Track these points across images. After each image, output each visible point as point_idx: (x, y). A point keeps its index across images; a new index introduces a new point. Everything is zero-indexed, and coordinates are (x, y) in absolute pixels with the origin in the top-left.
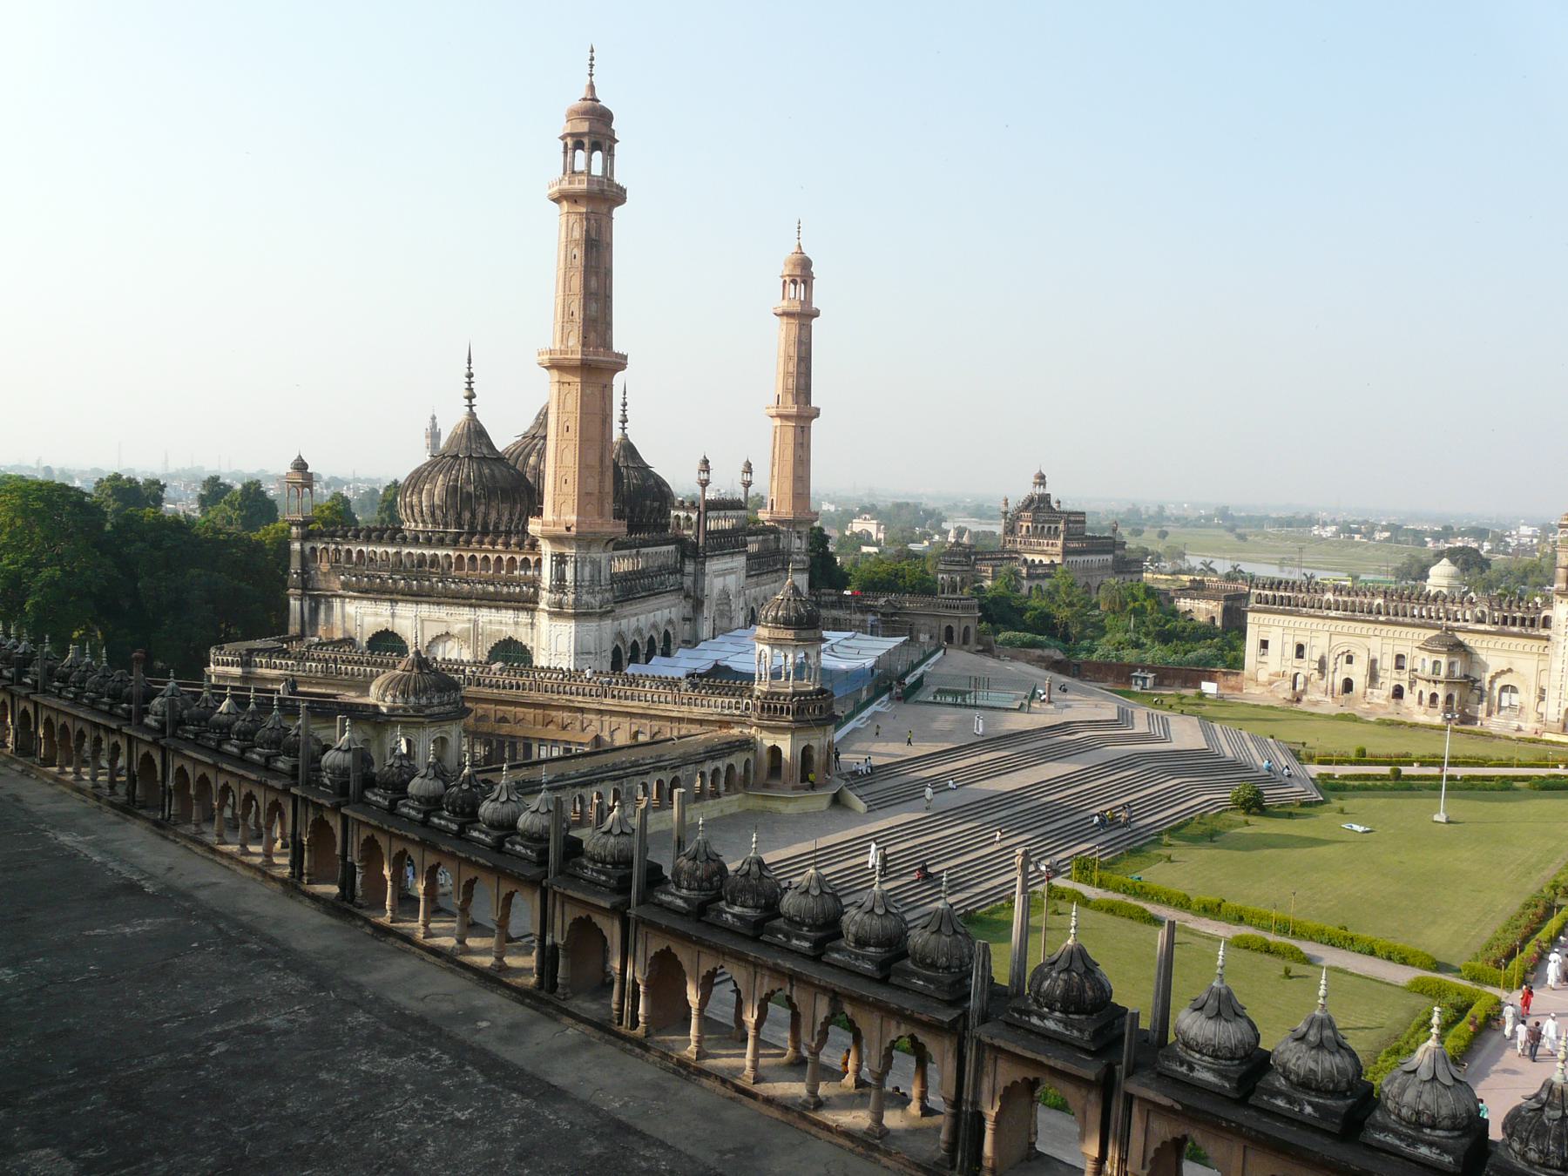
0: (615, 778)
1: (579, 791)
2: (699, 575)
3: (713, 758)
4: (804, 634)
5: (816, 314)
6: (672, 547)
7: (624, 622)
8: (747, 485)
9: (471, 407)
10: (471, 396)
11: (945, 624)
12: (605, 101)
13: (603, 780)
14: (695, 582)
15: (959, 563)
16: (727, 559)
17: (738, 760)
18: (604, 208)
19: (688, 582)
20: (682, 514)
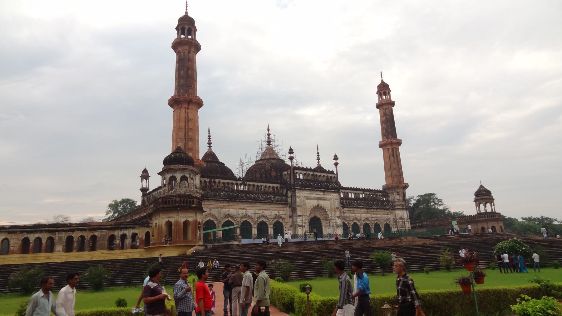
0: (49, 231)
1: (25, 235)
2: (294, 196)
3: (121, 229)
4: (172, 167)
5: (393, 104)
6: (276, 185)
7: (231, 210)
8: (336, 164)
9: (210, 147)
10: (210, 144)
11: (480, 227)
12: (190, 15)
13: (41, 232)
14: (292, 200)
15: (482, 195)
16: (318, 193)
17: (141, 232)
18: (186, 48)
19: (289, 200)
20: (286, 173)
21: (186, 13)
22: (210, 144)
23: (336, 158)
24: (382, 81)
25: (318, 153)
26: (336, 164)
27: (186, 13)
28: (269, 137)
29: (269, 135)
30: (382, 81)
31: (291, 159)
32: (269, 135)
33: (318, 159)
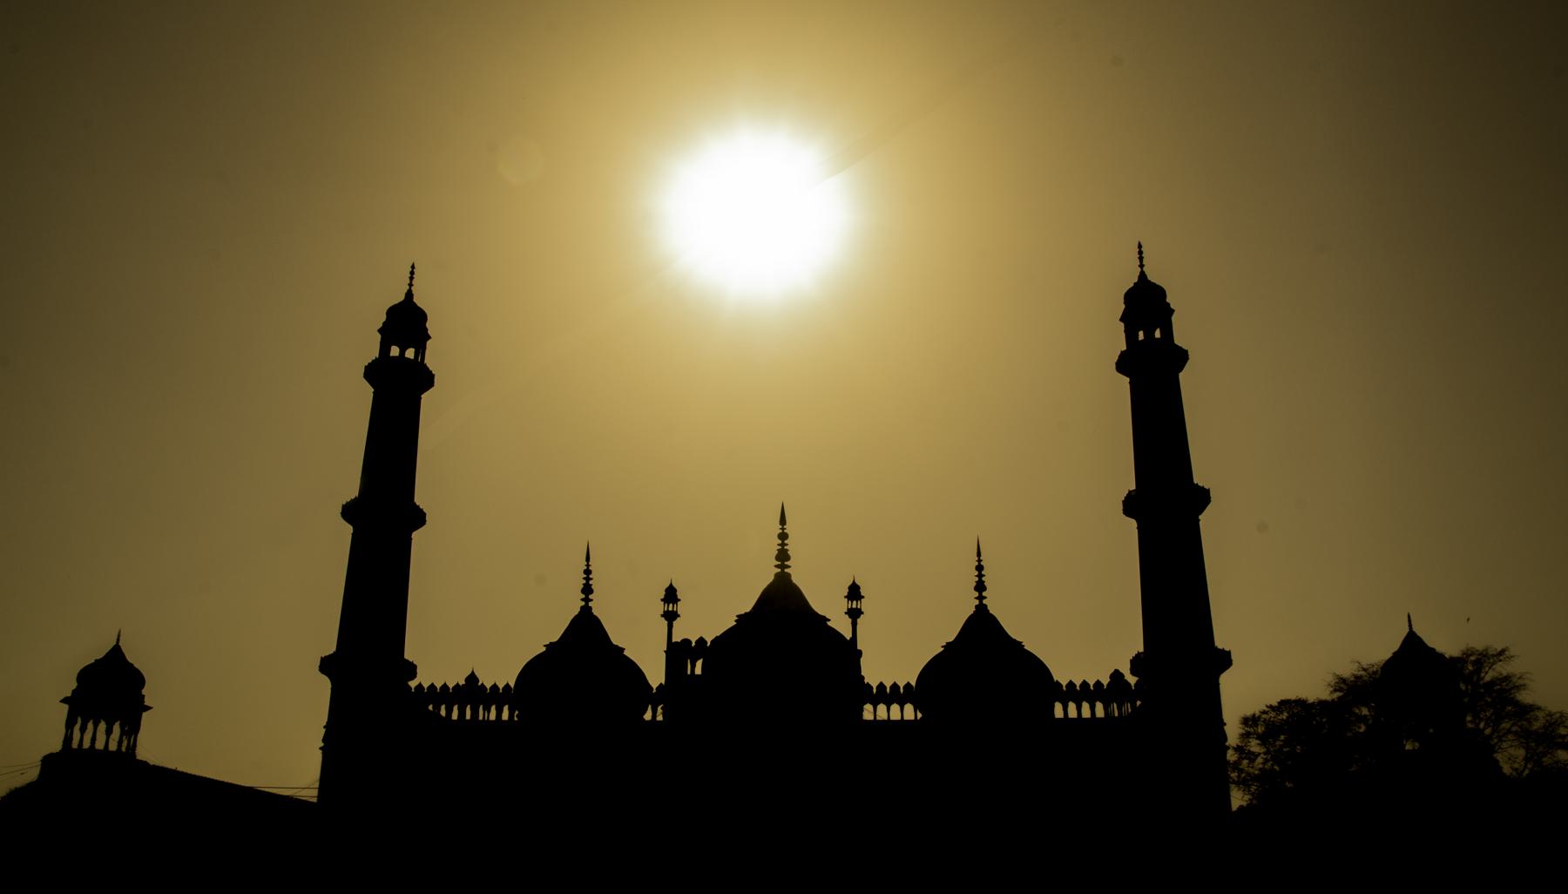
8: (854, 614)
9: (587, 600)
10: (587, 590)
21: (409, 295)
22: (587, 590)
23: (854, 592)
24: (1143, 276)
25: (980, 568)
26: (854, 614)
27: (409, 295)
28: (783, 545)
29: (783, 536)
30: (1143, 276)
31: (671, 617)
32: (783, 536)
33: (980, 587)
